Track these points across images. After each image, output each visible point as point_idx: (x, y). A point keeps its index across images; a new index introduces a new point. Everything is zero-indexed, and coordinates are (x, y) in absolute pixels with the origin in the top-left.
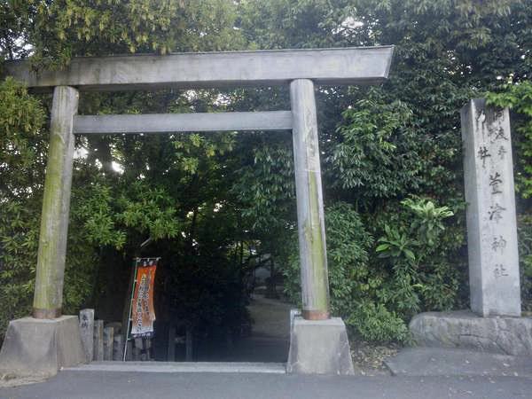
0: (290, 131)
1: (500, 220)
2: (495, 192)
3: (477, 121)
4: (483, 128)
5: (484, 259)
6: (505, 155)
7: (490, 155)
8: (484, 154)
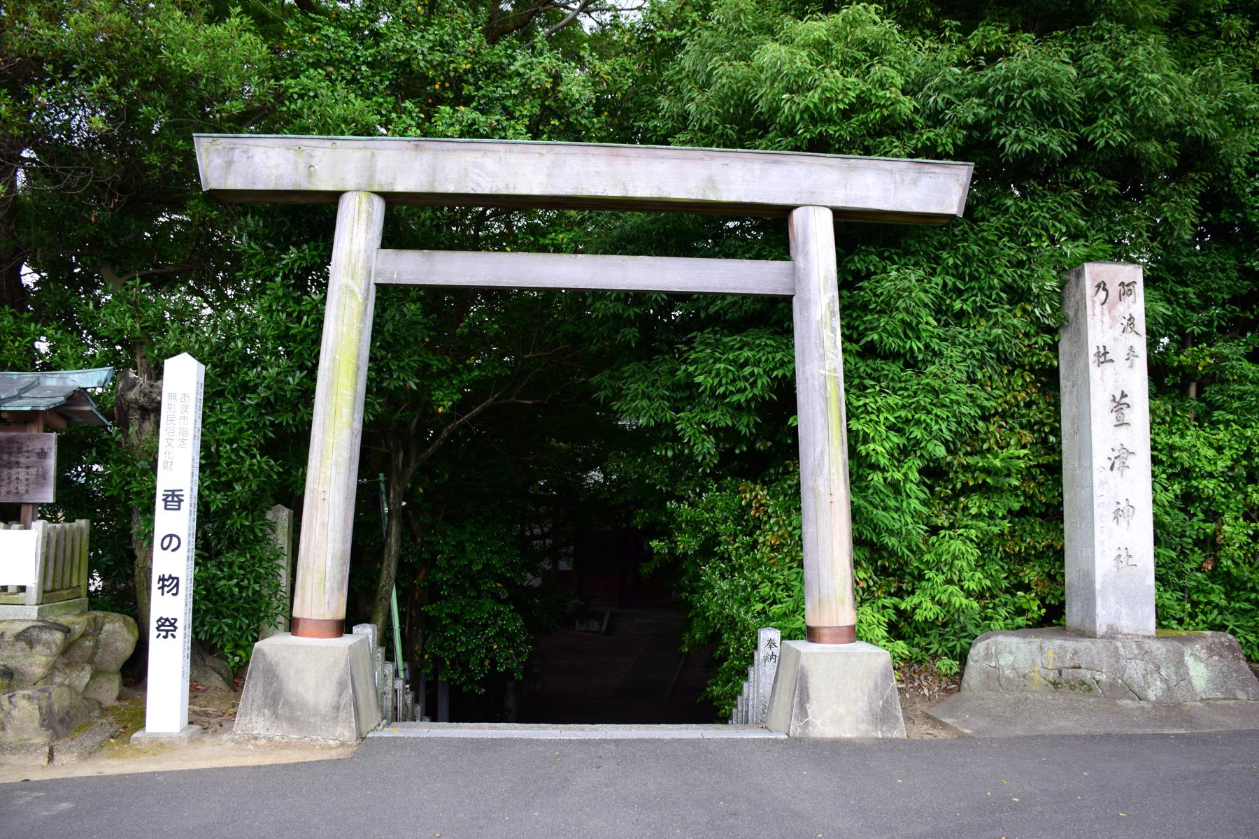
0: (788, 300)
1: (1126, 471)
2: (1121, 424)
3: (1093, 302)
4: (1102, 314)
5: (1098, 537)
6: (1137, 361)
7: (1111, 361)
8: (1103, 484)
